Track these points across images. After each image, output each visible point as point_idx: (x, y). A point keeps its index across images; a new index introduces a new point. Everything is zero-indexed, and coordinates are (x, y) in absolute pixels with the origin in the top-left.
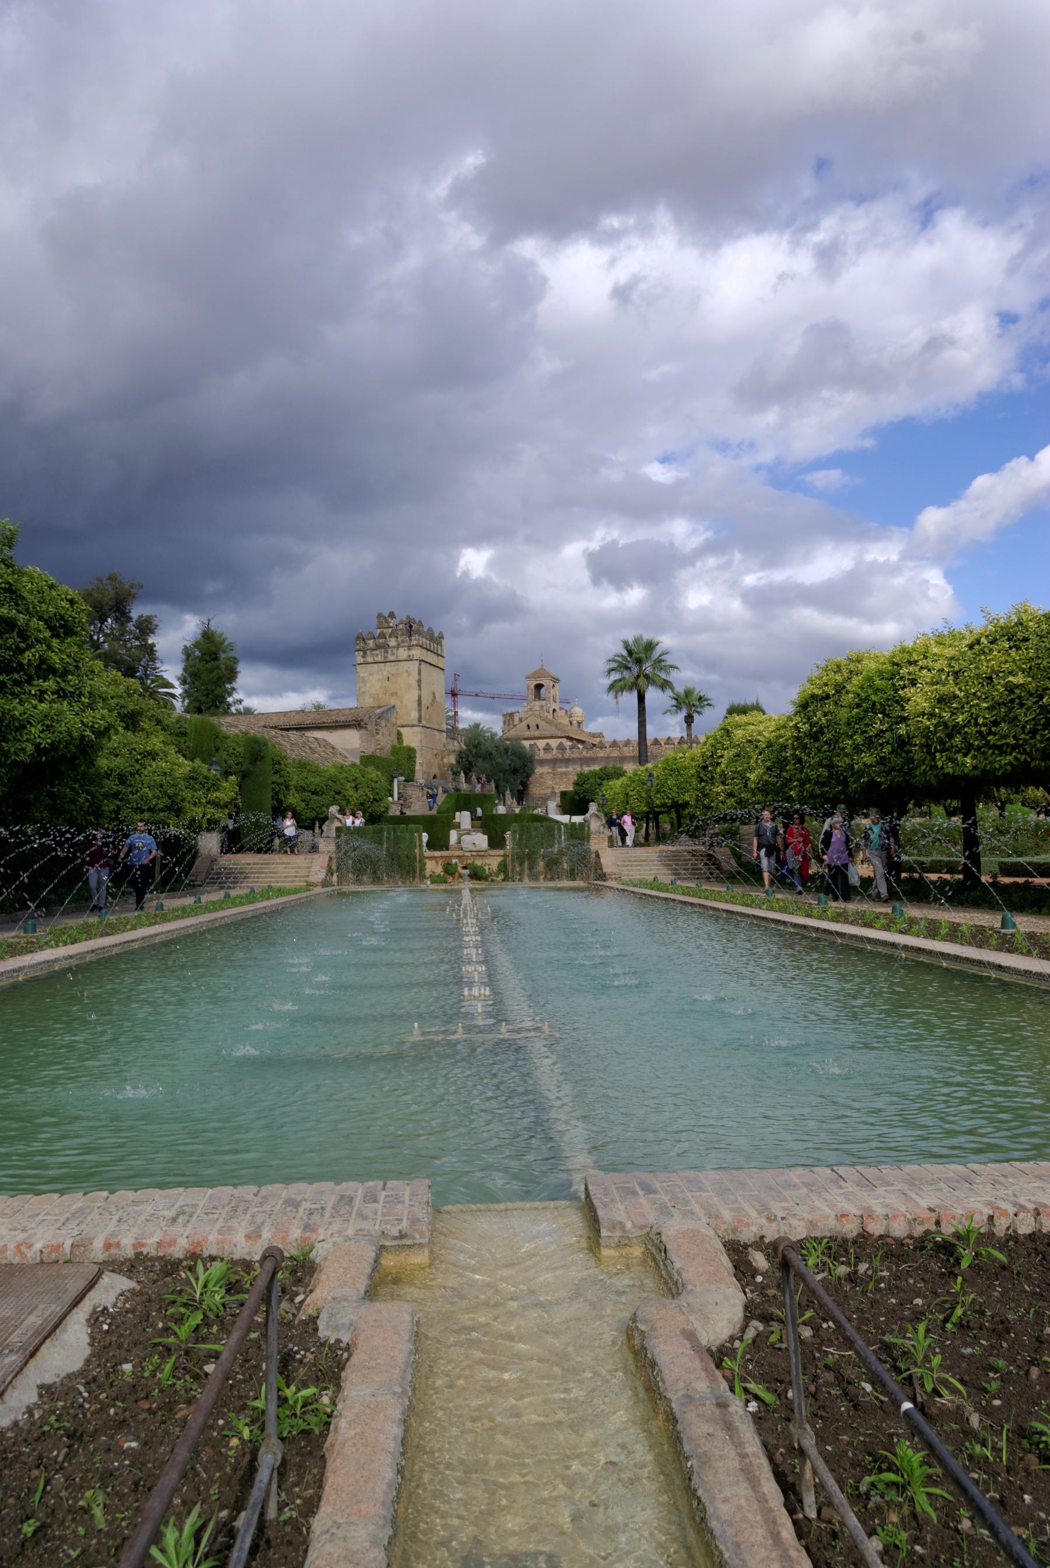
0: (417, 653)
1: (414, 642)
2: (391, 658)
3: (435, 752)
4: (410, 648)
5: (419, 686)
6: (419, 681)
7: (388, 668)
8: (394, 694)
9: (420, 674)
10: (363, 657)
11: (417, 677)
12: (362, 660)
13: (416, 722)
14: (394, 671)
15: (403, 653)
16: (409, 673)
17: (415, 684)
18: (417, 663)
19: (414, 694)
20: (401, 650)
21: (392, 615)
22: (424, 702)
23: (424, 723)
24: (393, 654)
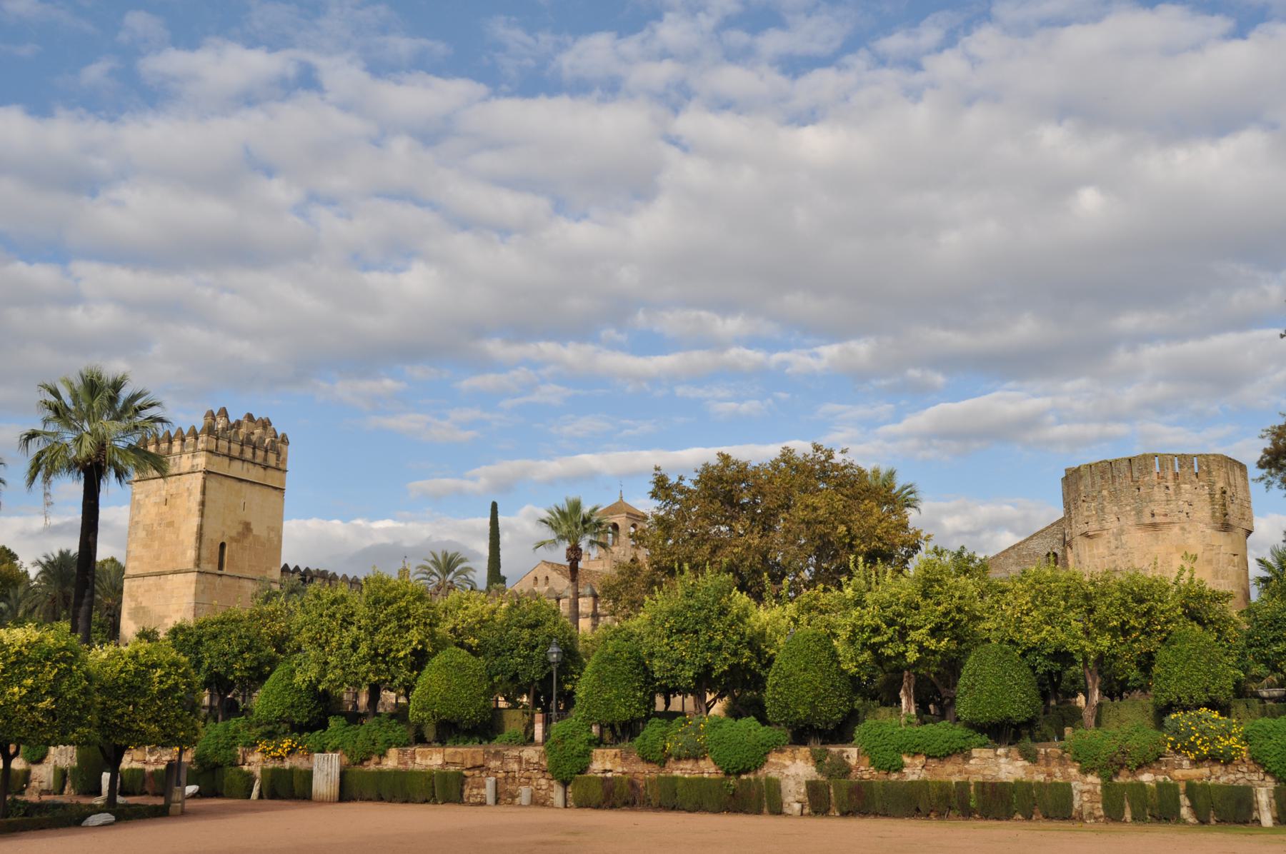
6: (203, 504)
8: (171, 524)
9: (204, 492)
11: (197, 496)
13: (191, 566)
14: (173, 491)
15: (185, 462)
17: (195, 507)
18: (200, 476)
19: (194, 521)
20: (185, 457)
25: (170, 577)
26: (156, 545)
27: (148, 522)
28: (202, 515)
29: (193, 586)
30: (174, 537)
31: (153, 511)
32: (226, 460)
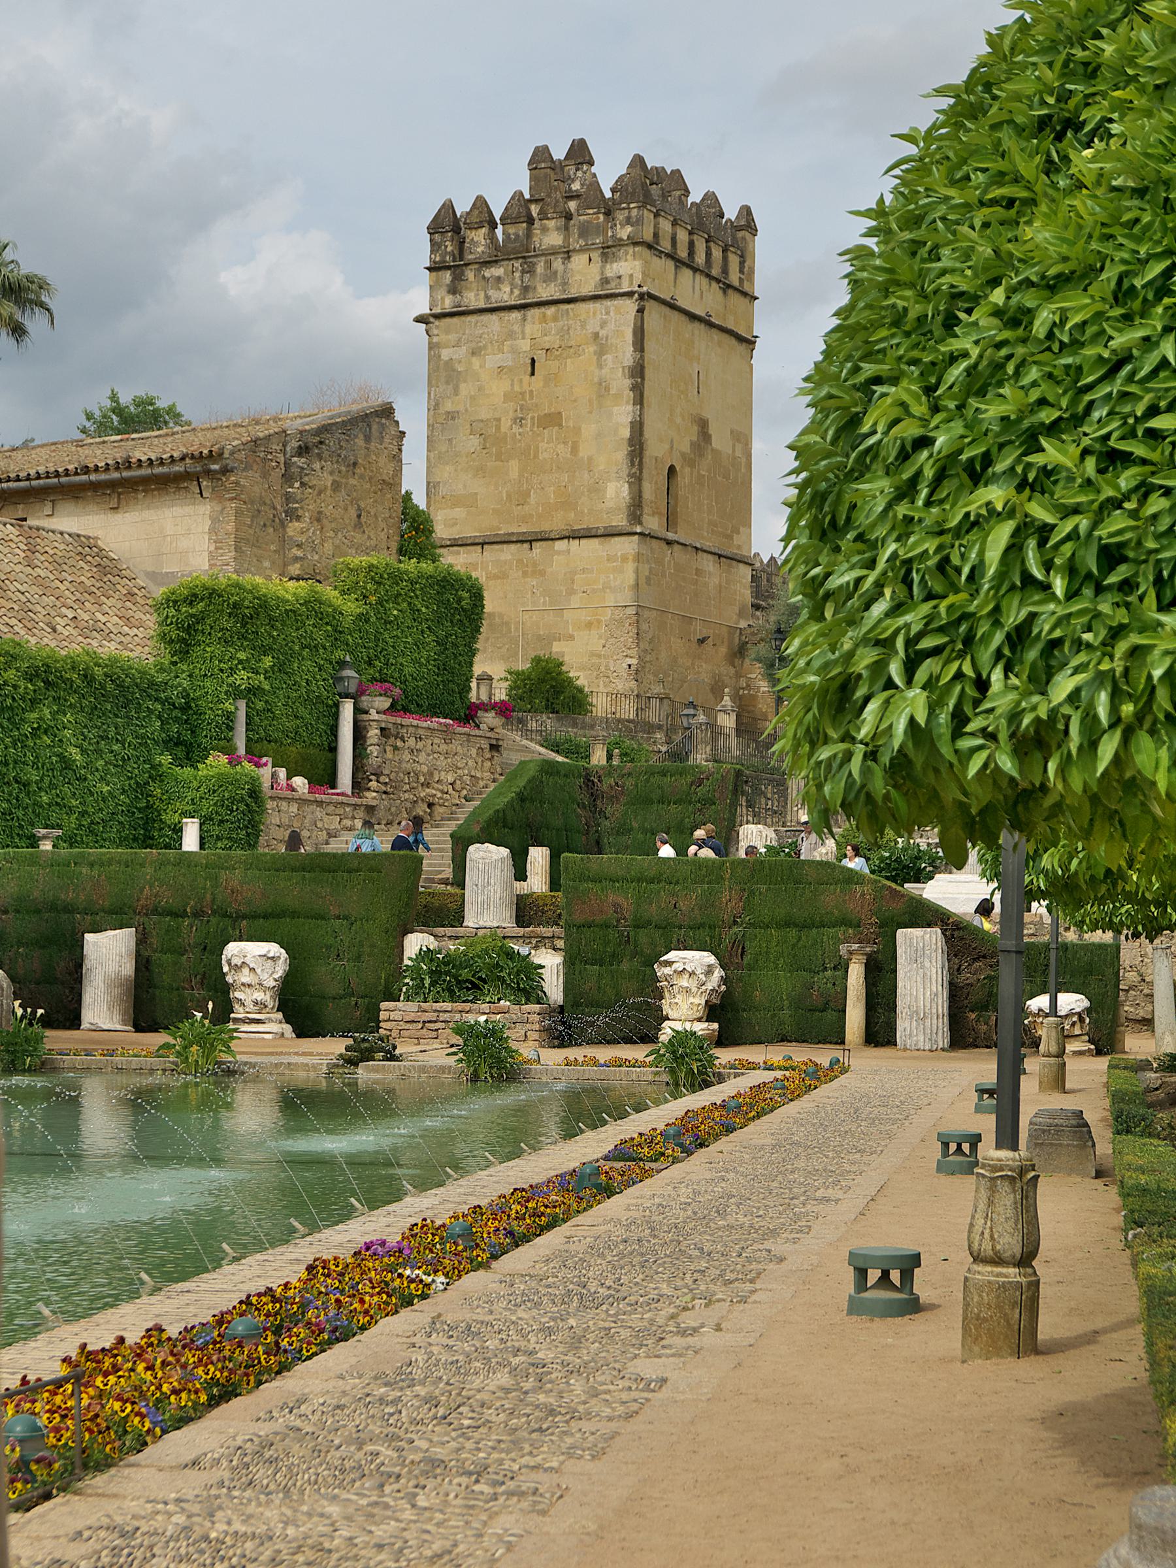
0: (629, 268)
1: (624, 232)
2: (545, 292)
3: (699, 631)
4: (609, 251)
5: (638, 391)
6: (638, 372)
7: (534, 329)
8: (552, 420)
10: (453, 290)
11: (627, 355)
12: (448, 303)
13: (620, 520)
15: (584, 273)
16: (602, 347)
18: (630, 307)
20: (579, 261)
21: (580, 153)
22: (655, 448)
23: (653, 523)
24: (551, 276)
25: (560, 545)
26: (514, 467)
27: (484, 414)
28: (639, 399)
29: (630, 567)
30: (564, 451)
31: (498, 388)
32: (670, 264)
